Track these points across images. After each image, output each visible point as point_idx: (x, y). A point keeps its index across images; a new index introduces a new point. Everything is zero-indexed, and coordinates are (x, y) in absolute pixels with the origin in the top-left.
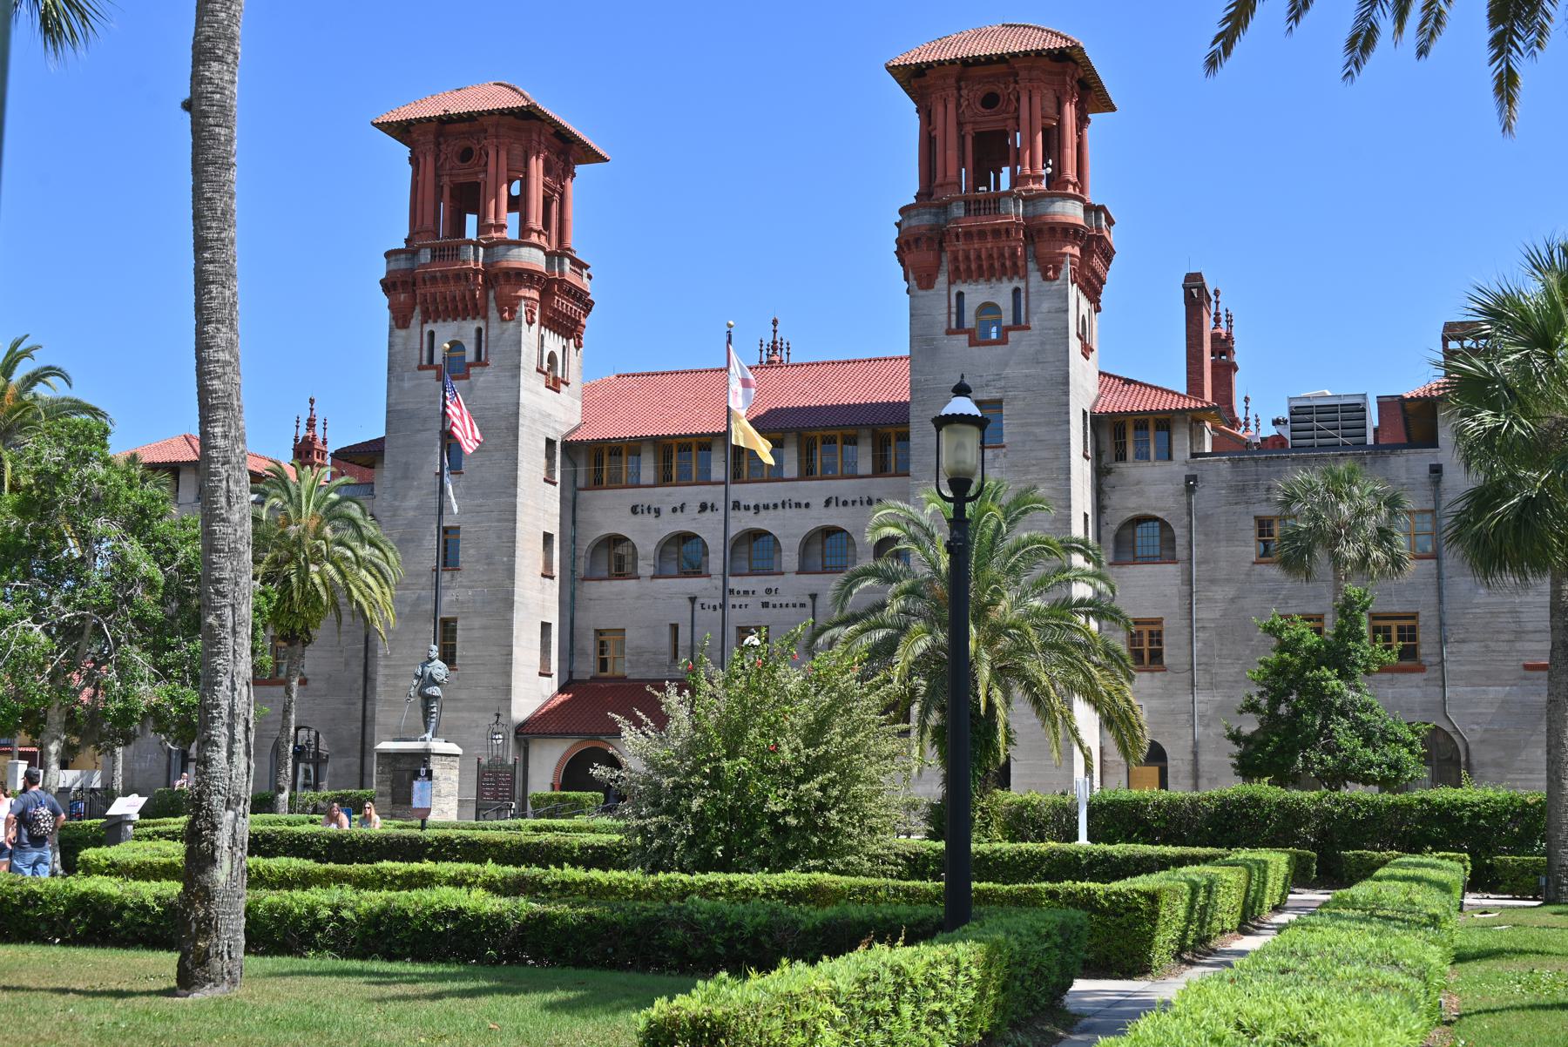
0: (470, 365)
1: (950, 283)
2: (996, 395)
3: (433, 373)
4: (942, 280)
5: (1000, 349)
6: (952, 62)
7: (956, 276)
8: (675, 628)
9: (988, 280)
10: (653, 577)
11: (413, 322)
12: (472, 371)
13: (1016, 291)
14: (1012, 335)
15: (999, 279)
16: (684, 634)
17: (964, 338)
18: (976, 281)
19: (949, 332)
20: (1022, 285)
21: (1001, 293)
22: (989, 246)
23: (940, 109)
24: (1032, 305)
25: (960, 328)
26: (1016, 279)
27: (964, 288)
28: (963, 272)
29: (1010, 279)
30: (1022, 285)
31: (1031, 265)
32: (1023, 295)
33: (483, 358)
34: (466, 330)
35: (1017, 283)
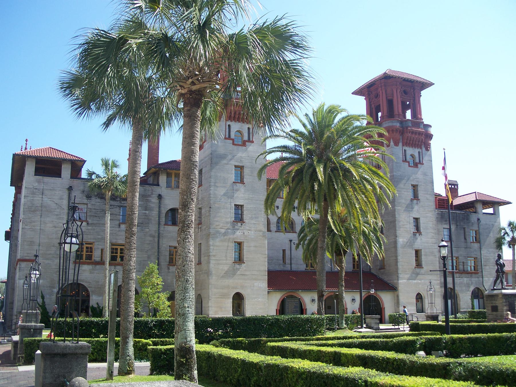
0: (246, 141)
1: (403, 145)
2: (417, 184)
3: (231, 141)
4: (400, 144)
5: (416, 169)
6: (402, 78)
7: (405, 144)
8: (284, 251)
9: (412, 147)
10: (276, 232)
11: (222, 119)
12: (247, 143)
13: (419, 152)
14: (419, 165)
15: (415, 147)
16: (288, 253)
17: (407, 164)
18: (410, 147)
19: (403, 161)
20: (421, 151)
21: (415, 152)
22: (417, 137)
23: (395, 91)
24: (423, 157)
25: (405, 161)
26: (419, 149)
27: (407, 148)
28: (407, 143)
29: (418, 148)
30: (421, 151)
31: (423, 146)
32: (421, 154)
33: (251, 139)
34: (244, 127)
35: (419, 150)
